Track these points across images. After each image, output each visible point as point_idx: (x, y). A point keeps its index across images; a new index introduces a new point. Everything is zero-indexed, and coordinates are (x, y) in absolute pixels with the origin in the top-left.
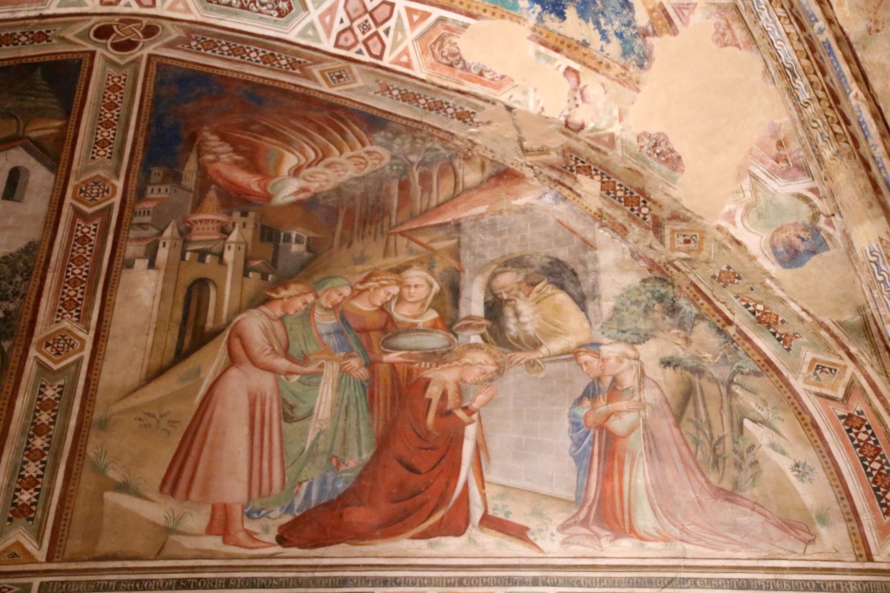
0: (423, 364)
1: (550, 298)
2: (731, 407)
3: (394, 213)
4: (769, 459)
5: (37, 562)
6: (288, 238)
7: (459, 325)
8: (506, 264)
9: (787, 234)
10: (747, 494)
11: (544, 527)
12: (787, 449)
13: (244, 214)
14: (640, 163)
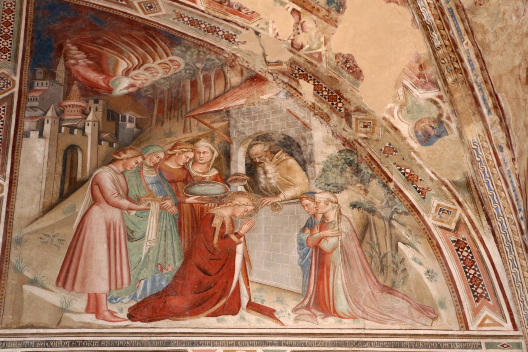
0: (210, 204)
1: (284, 162)
2: (391, 234)
4: (412, 267)
7: (230, 179)
8: (257, 139)
9: (424, 124)
11: (284, 310)
12: (422, 261)
13: (96, 102)
14: (337, 73)
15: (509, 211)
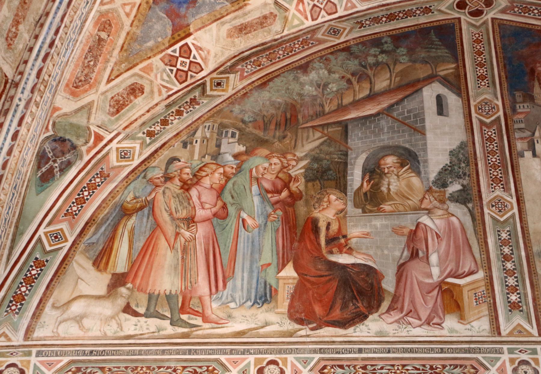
5: (533, 336)
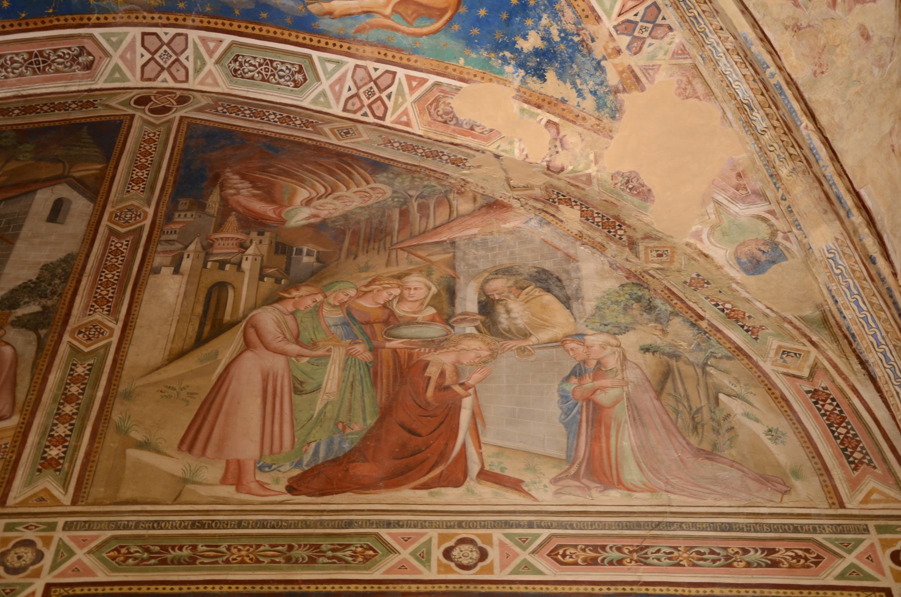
0: (423, 350)
1: (538, 299)
2: (706, 384)
3: (395, 233)
5: (62, 505)
6: (300, 252)
7: (455, 319)
8: (497, 273)
10: (726, 453)
11: (537, 480)
13: (261, 234)
14: (615, 196)
15: (895, 336)
